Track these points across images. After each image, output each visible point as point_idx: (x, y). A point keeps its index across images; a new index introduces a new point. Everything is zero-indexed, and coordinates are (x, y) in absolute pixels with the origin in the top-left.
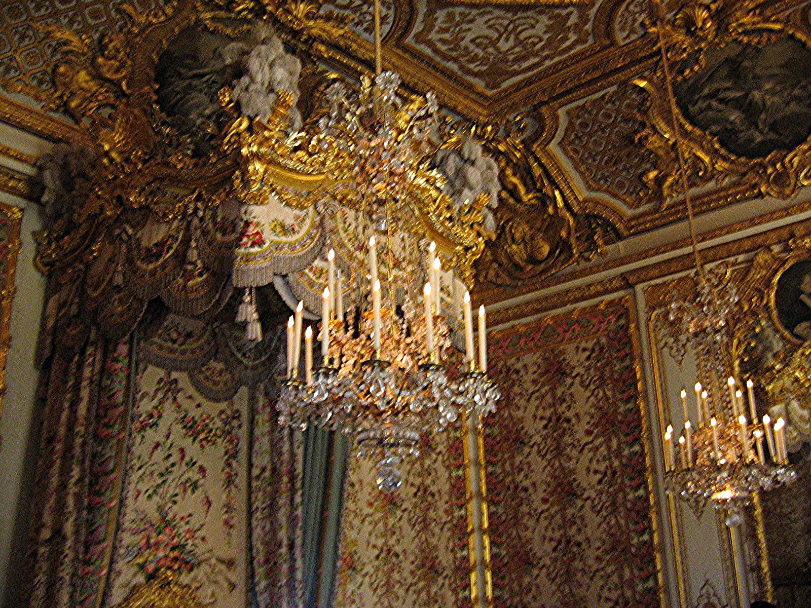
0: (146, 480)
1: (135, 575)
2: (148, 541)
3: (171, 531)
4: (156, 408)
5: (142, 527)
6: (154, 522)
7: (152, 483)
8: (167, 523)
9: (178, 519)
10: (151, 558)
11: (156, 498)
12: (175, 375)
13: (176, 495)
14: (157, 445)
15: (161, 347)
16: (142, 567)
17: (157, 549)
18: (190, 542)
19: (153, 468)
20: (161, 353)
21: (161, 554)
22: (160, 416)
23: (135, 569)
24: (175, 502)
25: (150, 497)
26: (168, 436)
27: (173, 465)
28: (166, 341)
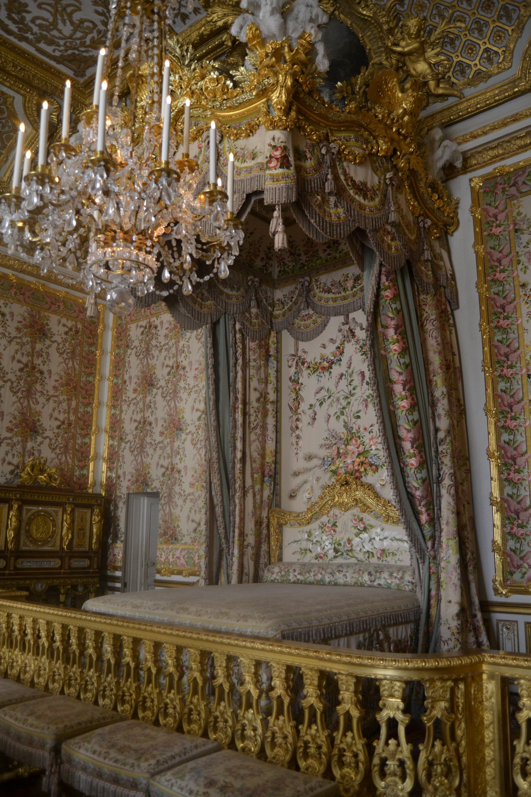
0: (334, 405)
1: (330, 478)
2: (338, 452)
3: (356, 441)
4: (338, 348)
5: (334, 442)
6: (342, 436)
7: (339, 406)
8: (352, 435)
9: (362, 430)
10: (341, 465)
11: (342, 417)
12: (351, 316)
13: (358, 412)
14: (342, 375)
15: (335, 300)
16: (334, 472)
17: (346, 457)
18: (373, 448)
19: (338, 395)
20: (335, 304)
21: (349, 461)
22: (342, 353)
23: (329, 474)
24: (359, 417)
25: (338, 417)
26: (349, 368)
27: (354, 389)
28: (340, 293)
